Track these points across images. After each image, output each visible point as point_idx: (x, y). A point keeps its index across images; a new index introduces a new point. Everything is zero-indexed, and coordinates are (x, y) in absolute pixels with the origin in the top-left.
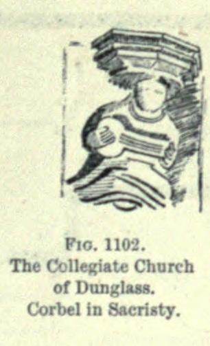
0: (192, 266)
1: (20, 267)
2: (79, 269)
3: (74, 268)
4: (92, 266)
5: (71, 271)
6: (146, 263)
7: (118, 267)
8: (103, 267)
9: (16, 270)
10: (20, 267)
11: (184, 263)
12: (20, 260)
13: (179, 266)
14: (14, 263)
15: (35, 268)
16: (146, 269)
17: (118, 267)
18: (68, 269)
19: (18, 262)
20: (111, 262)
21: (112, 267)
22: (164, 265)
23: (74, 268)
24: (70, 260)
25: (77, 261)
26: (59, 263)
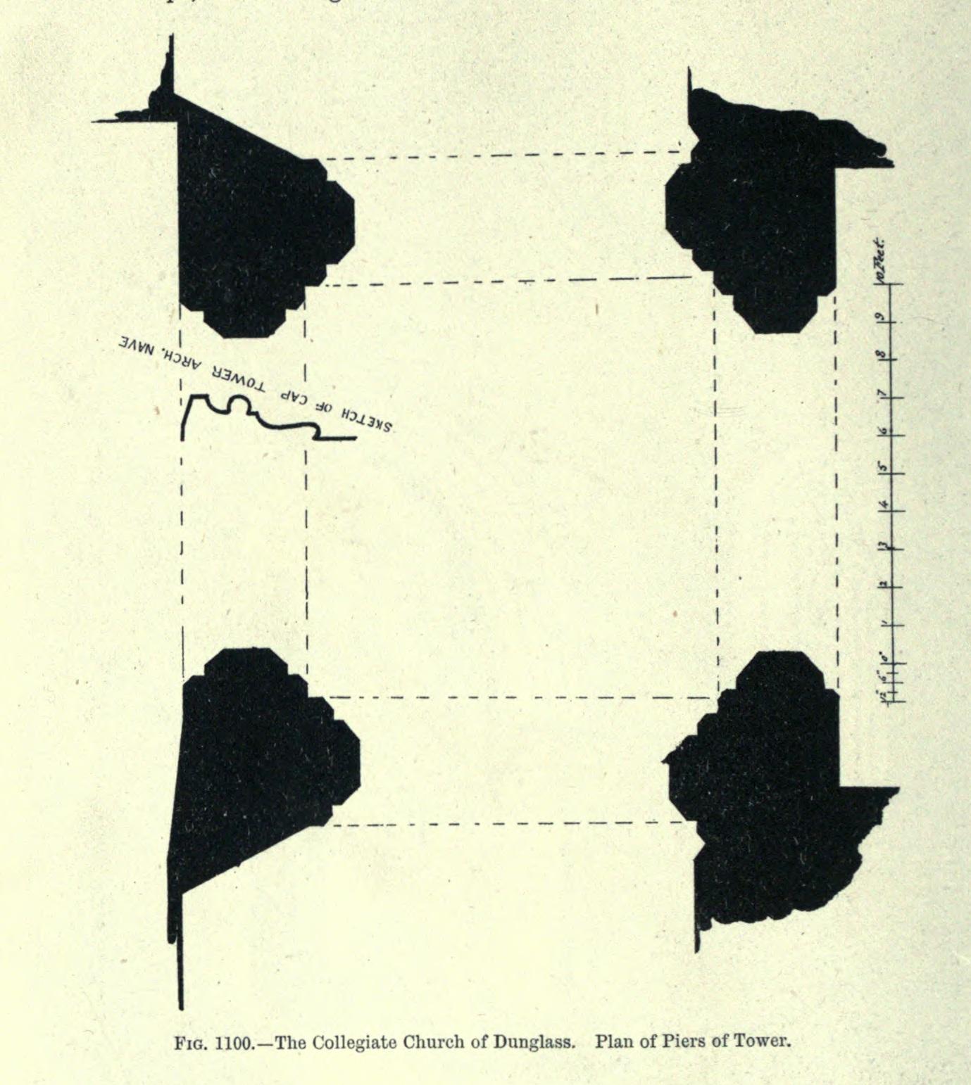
0: (462, 1041)
1: (285, 1044)
2: (346, 1045)
3: (340, 1045)
4: (360, 1042)
5: (337, 1047)
6: (416, 1038)
7: (386, 1043)
8: (371, 1044)
9: (281, 1047)
10: (285, 1044)
11: (454, 1039)
12: (285, 1037)
13: (450, 1041)
14: (278, 1039)
15: (302, 1044)
16: (416, 1045)
17: (386, 1043)
18: (335, 1046)
19: (283, 1039)
20: (379, 1039)
21: (380, 1043)
22: (434, 1040)
23: (340, 1045)
24: (337, 1037)
25: (343, 1037)
26: (325, 1039)
